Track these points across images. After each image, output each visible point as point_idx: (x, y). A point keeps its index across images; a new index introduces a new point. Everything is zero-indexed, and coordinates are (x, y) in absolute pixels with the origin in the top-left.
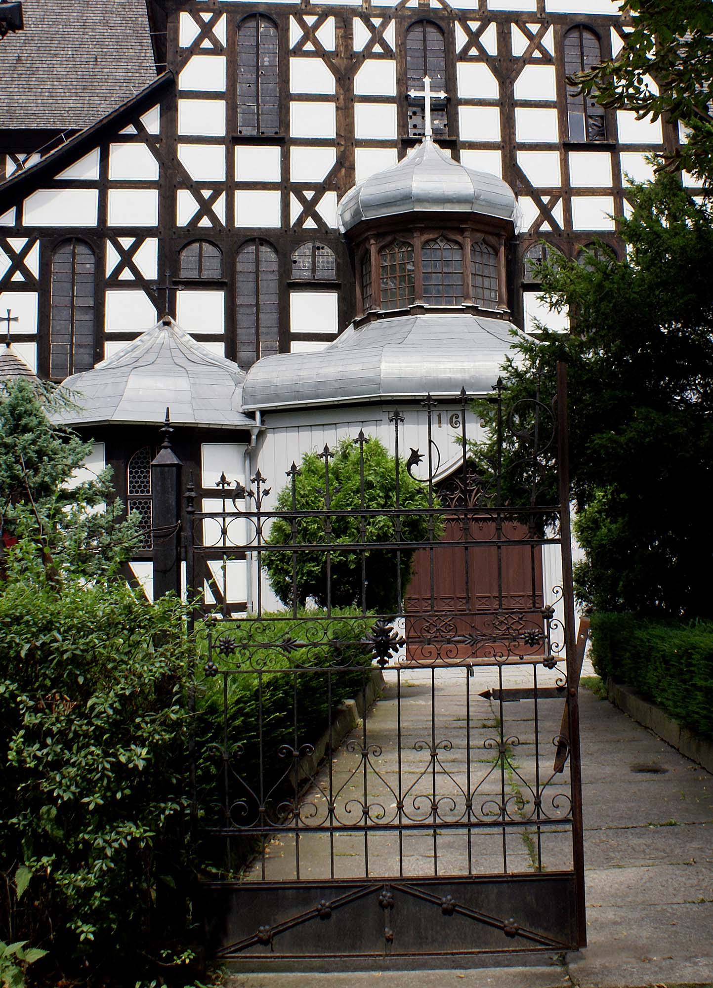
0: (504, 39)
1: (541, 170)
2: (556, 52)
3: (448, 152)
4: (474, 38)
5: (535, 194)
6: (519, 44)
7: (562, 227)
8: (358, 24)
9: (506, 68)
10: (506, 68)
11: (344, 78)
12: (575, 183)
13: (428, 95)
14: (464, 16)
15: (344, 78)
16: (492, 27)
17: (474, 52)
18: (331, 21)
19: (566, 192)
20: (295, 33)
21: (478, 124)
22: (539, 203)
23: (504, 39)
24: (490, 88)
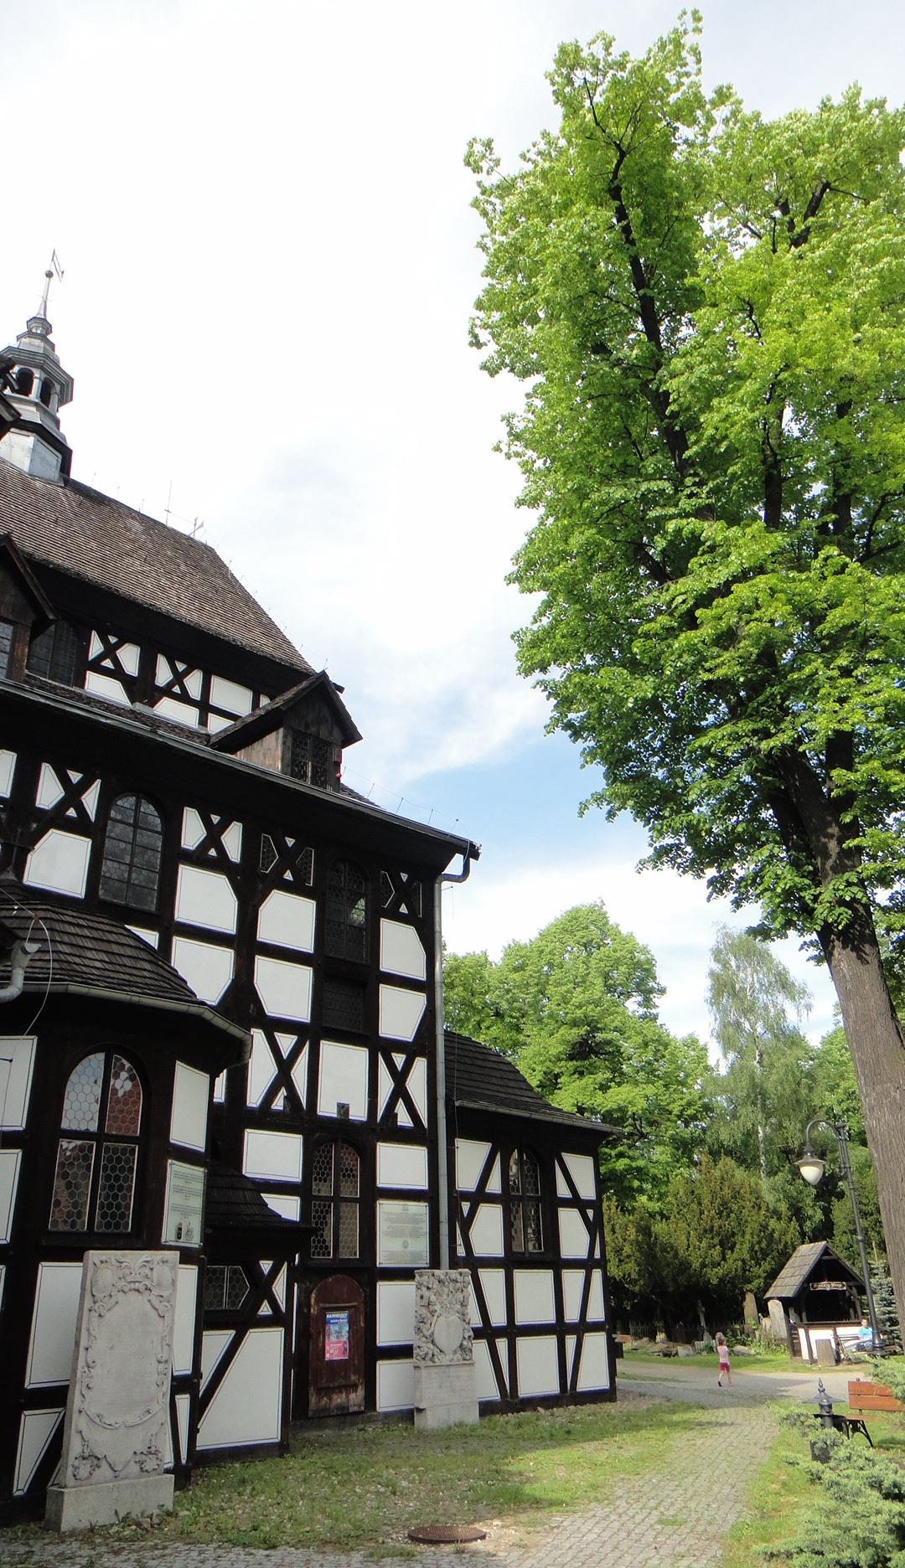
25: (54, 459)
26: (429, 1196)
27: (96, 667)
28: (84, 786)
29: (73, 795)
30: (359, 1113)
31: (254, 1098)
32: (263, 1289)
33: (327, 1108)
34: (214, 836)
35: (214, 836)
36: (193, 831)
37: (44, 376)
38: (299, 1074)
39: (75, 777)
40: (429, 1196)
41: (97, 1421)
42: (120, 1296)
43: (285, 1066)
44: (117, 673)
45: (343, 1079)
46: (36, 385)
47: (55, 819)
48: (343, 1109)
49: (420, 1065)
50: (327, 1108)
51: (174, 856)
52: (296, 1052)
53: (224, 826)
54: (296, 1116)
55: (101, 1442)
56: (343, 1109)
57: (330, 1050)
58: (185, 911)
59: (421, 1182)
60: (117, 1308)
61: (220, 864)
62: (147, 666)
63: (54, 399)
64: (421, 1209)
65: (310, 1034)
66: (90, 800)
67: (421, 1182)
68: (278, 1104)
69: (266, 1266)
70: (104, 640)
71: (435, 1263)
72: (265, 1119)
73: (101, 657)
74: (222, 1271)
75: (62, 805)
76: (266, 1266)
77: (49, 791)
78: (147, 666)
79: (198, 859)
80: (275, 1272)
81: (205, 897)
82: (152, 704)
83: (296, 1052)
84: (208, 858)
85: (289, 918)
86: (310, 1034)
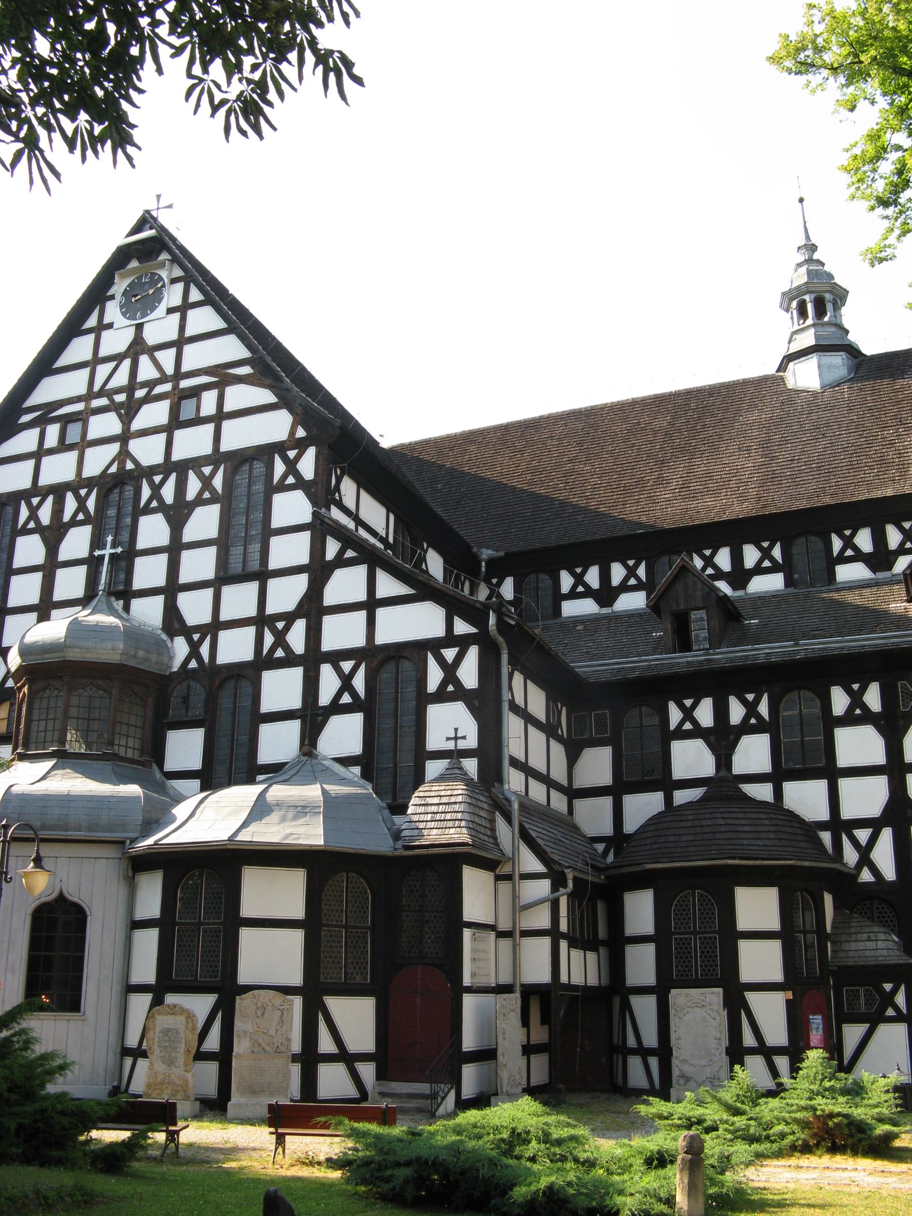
1: (195, 608)
2: (223, 489)
3: (121, 602)
5: (187, 631)
7: (206, 660)
8: (70, 497)
9: (178, 515)
11: (52, 548)
12: (252, 612)
13: (107, 552)
14: (152, 470)
15: (52, 548)
18: (50, 499)
19: (216, 626)
20: (24, 513)
21: (149, 572)
22: (190, 641)
25: (838, 360)
27: (843, 560)
28: (757, 701)
29: (751, 709)
34: (857, 699)
35: (857, 699)
36: (840, 701)
37: (813, 296)
39: (750, 697)
41: (685, 1061)
42: (690, 1010)
44: (859, 557)
46: (810, 307)
47: (745, 728)
51: (831, 723)
53: (863, 690)
55: (688, 1070)
58: (844, 760)
60: (688, 1015)
61: (867, 717)
62: (879, 538)
63: (829, 307)
66: (763, 708)
69: (888, 987)
70: (841, 536)
73: (843, 550)
74: (858, 991)
75: (746, 719)
76: (888, 987)
77: (736, 712)
78: (879, 538)
79: (849, 720)
80: (895, 991)
81: (858, 745)
82: (890, 567)
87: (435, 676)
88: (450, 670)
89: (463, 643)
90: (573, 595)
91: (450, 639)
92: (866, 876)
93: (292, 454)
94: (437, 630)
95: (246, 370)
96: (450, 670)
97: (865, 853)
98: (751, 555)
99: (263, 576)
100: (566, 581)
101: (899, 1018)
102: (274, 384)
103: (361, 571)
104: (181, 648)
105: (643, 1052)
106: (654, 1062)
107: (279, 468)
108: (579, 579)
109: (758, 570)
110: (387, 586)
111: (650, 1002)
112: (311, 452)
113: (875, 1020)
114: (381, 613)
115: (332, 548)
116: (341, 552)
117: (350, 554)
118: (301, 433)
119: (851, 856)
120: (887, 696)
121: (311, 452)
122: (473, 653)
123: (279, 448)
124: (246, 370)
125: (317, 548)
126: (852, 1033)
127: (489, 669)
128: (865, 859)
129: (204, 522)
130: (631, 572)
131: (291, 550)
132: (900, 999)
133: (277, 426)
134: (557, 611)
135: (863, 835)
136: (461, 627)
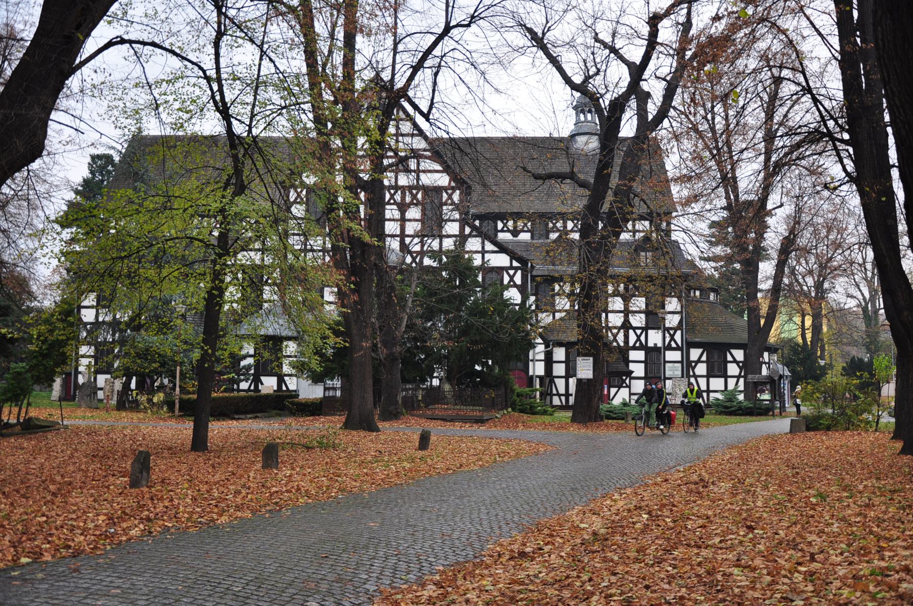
0: (403, 198)
4: (392, 196)
6: (408, 199)
9: (403, 207)
10: (403, 207)
16: (399, 192)
17: (392, 201)
19: (422, 253)
23: (403, 198)
24: (397, 214)
26: (681, 362)
30: (660, 345)
31: (631, 344)
32: (624, 381)
33: (651, 344)
38: (643, 338)
40: (681, 362)
43: (639, 337)
45: (655, 338)
48: (655, 344)
49: (679, 332)
50: (651, 344)
52: (641, 334)
54: (644, 347)
56: (655, 344)
57: (650, 331)
59: (679, 359)
64: (679, 365)
65: (645, 329)
67: (679, 359)
68: (638, 345)
71: (683, 377)
72: (634, 348)
83: (641, 334)
84: (616, 294)
85: (639, 303)
86: (645, 329)
87: (506, 279)
88: (512, 278)
89: (516, 269)
90: (502, 231)
91: (511, 267)
92: (615, 344)
93: (450, 192)
94: (508, 265)
95: (428, 153)
96: (512, 278)
97: (615, 336)
98: (570, 225)
99: (441, 237)
100: (500, 225)
101: (627, 386)
102: (442, 162)
103: (479, 239)
104: (409, 260)
105: (559, 395)
106: (563, 398)
107: (445, 196)
108: (505, 225)
109: (572, 231)
110: (489, 246)
111: (564, 380)
112: (458, 192)
113: (620, 387)
114: (486, 255)
115: (467, 230)
116: (471, 232)
117: (474, 233)
118: (453, 184)
119: (611, 337)
120: (626, 289)
121: (458, 192)
122: (519, 273)
123: (445, 189)
124: (428, 153)
125: (462, 229)
126: (613, 391)
127: (524, 277)
128: (615, 340)
129: (414, 213)
130: (525, 225)
131: (452, 228)
132: (627, 381)
133: (443, 180)
134: (496, 235)
135: (615, 331)
136: (515, 264)
